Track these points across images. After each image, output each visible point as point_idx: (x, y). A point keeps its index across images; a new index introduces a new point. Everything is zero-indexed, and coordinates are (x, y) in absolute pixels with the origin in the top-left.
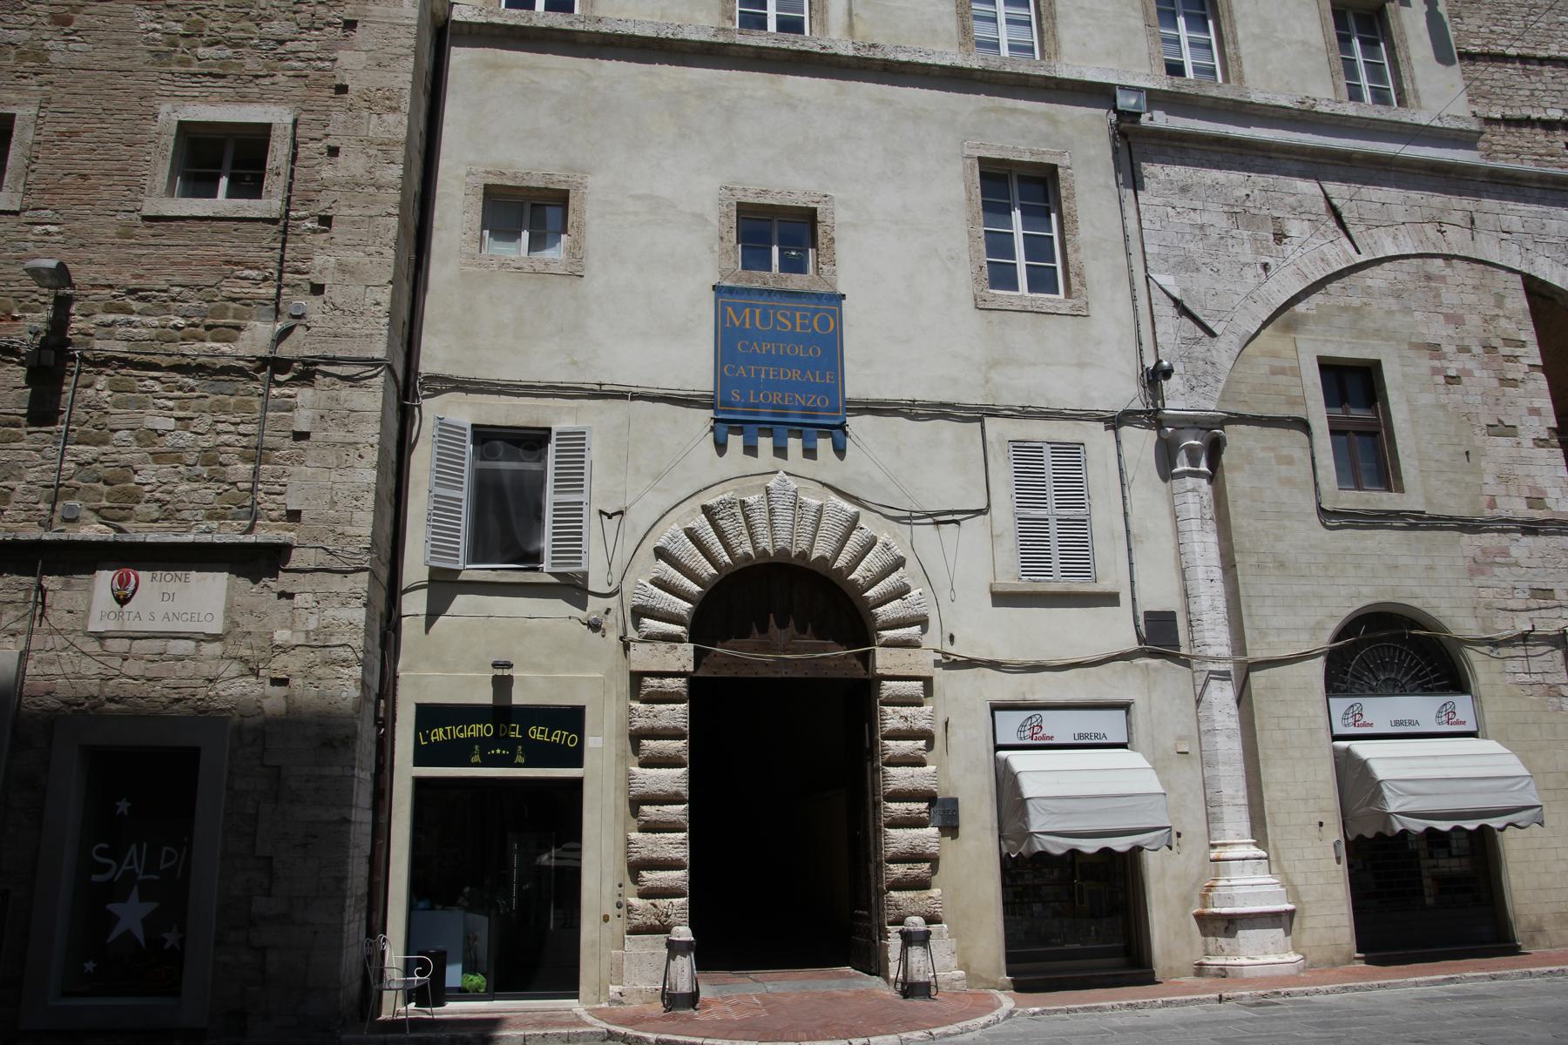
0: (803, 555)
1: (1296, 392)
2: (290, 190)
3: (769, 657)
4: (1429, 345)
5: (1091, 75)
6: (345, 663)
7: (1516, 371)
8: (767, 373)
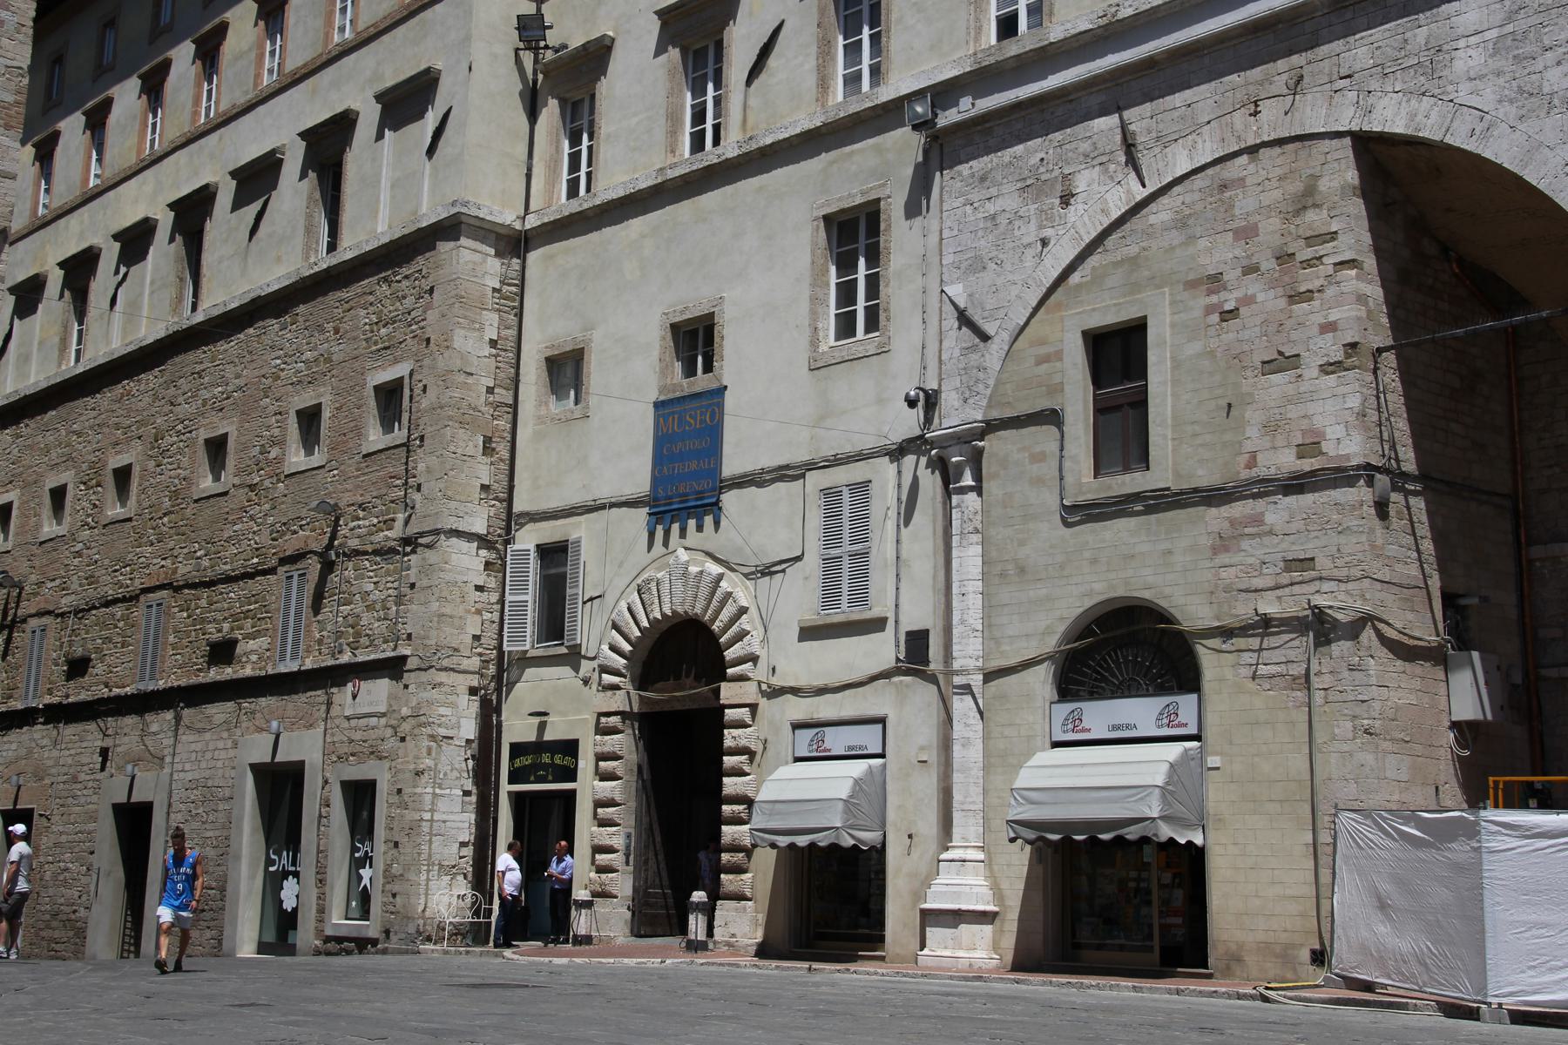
1: (1057, 379)
4: (1209, 277)
7: (1310, 280)
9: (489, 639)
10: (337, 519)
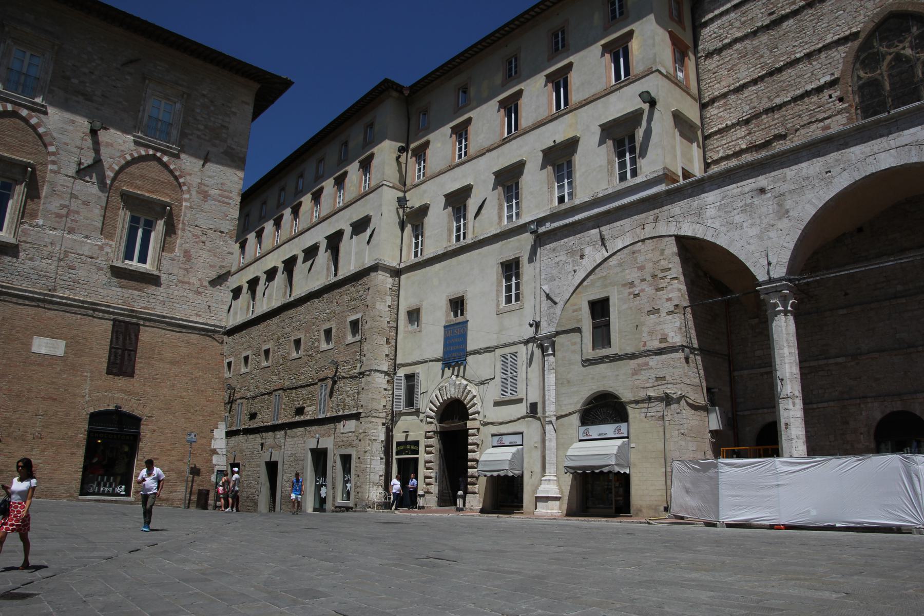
1: (580, 317)
4: (630, 283)
7: (663, 284)
9: (389, 407)
10: (338, 366)
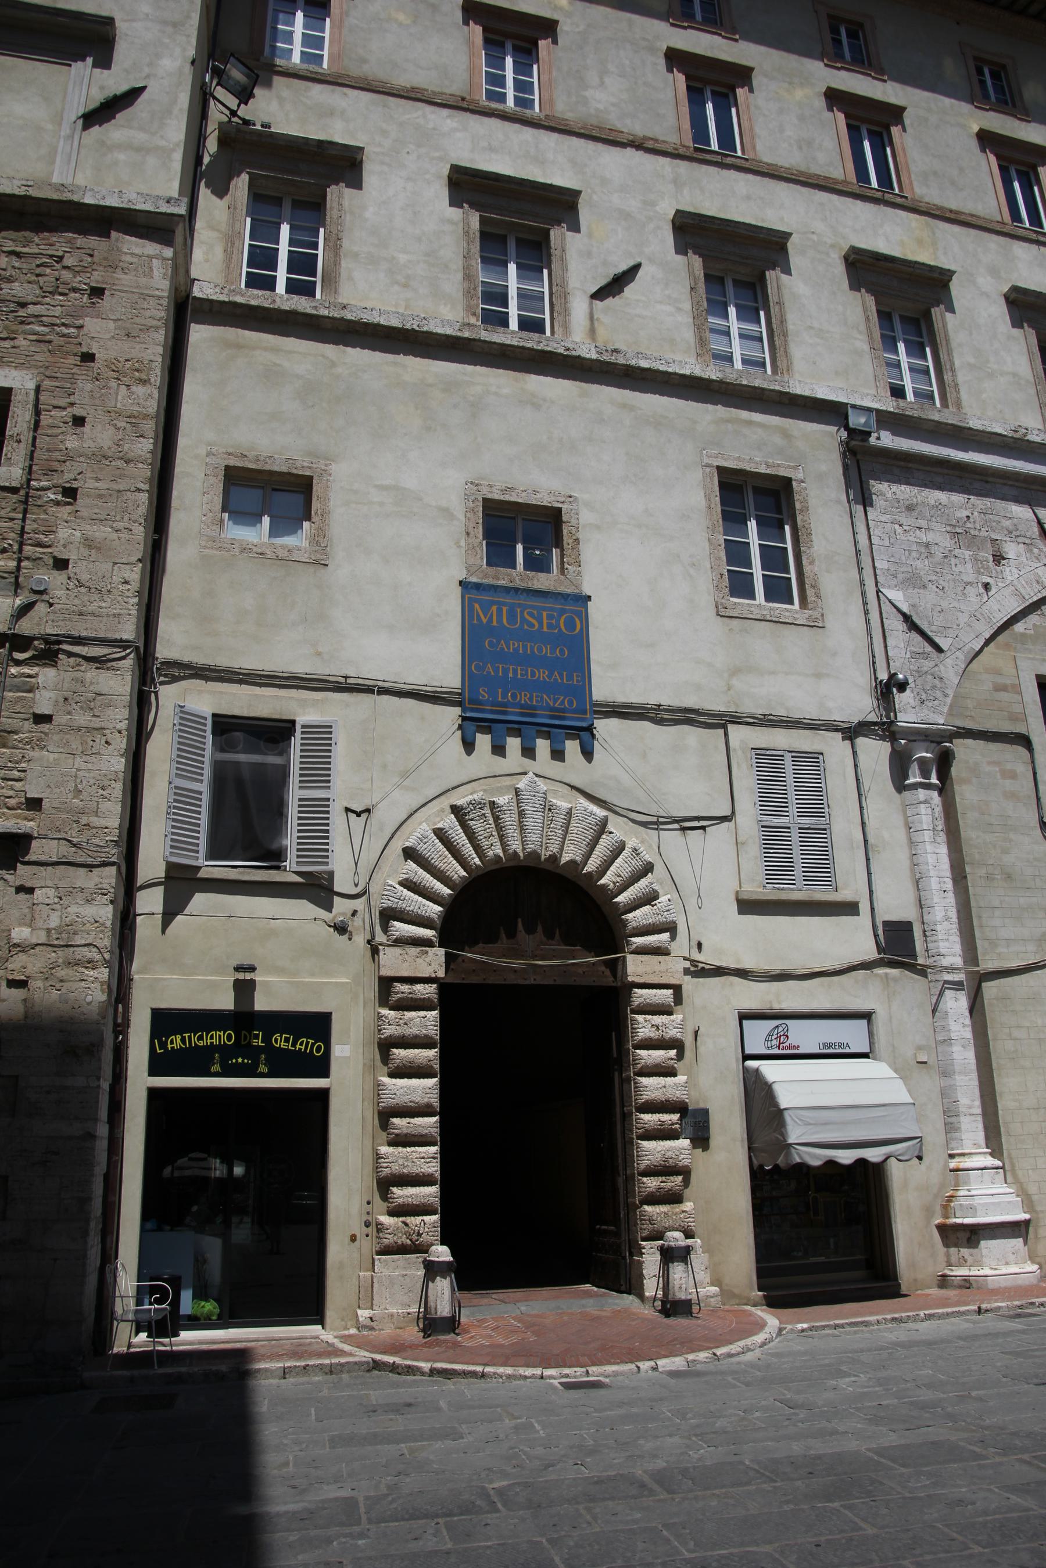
0: (554, 859)
1: (1017, 709)
2: (32, 458)
3: (519, 964)
5: (823, 393)
6: (90, 964)
8: (515, 672)
